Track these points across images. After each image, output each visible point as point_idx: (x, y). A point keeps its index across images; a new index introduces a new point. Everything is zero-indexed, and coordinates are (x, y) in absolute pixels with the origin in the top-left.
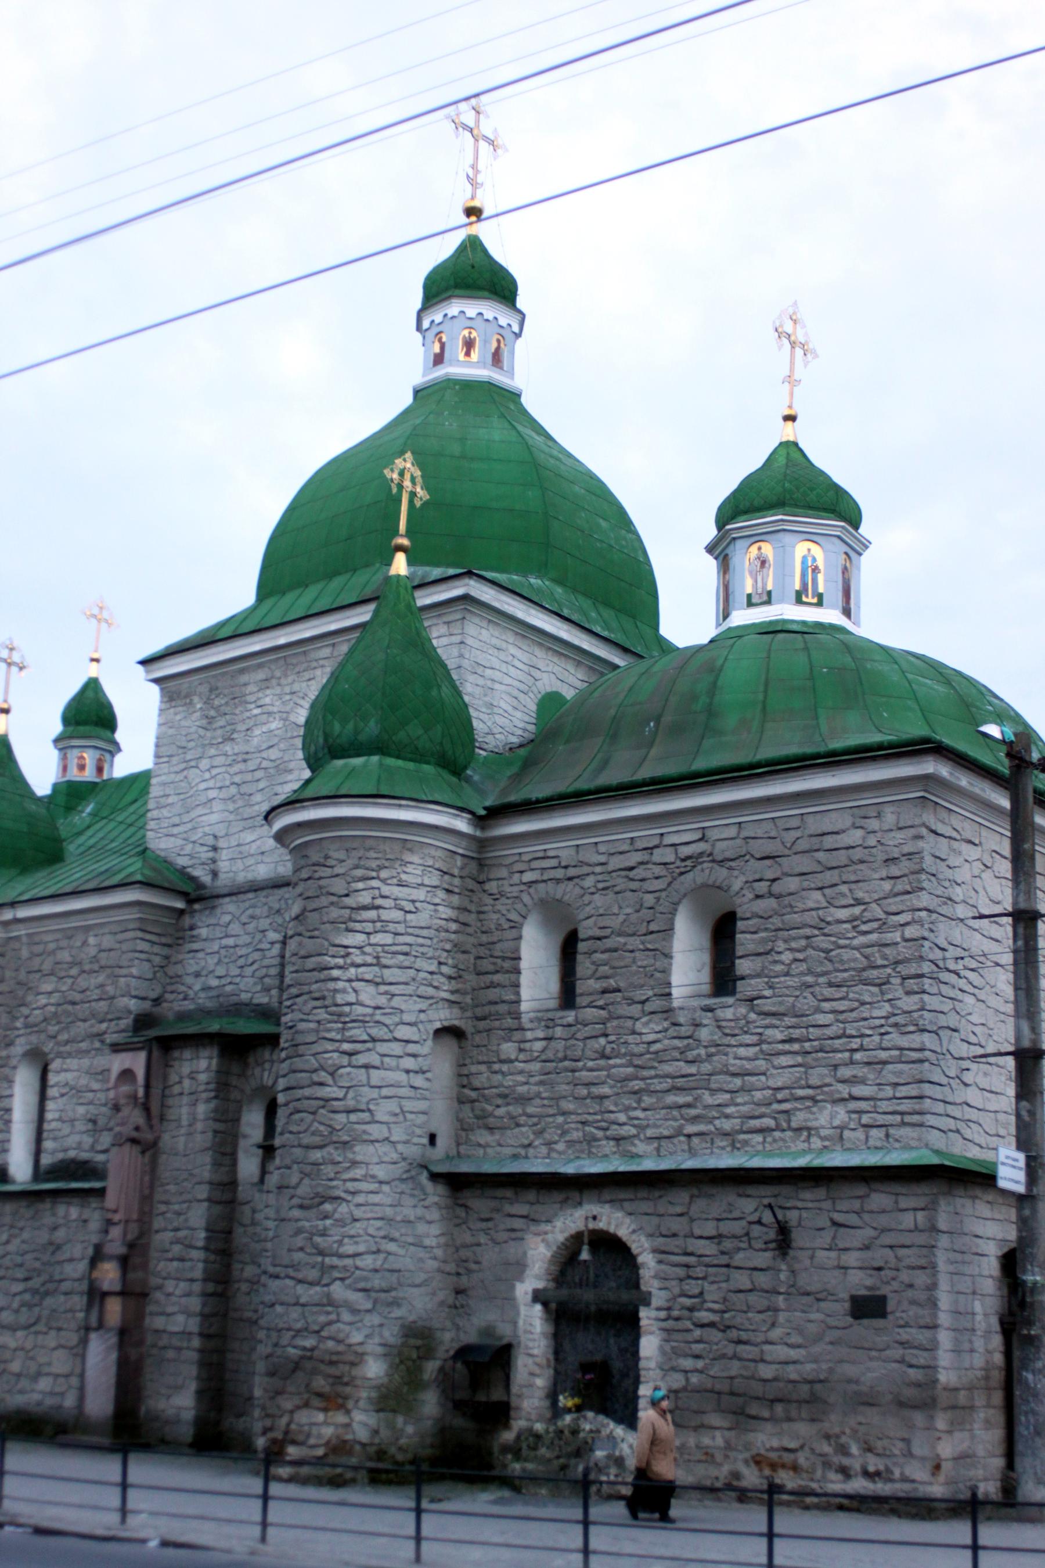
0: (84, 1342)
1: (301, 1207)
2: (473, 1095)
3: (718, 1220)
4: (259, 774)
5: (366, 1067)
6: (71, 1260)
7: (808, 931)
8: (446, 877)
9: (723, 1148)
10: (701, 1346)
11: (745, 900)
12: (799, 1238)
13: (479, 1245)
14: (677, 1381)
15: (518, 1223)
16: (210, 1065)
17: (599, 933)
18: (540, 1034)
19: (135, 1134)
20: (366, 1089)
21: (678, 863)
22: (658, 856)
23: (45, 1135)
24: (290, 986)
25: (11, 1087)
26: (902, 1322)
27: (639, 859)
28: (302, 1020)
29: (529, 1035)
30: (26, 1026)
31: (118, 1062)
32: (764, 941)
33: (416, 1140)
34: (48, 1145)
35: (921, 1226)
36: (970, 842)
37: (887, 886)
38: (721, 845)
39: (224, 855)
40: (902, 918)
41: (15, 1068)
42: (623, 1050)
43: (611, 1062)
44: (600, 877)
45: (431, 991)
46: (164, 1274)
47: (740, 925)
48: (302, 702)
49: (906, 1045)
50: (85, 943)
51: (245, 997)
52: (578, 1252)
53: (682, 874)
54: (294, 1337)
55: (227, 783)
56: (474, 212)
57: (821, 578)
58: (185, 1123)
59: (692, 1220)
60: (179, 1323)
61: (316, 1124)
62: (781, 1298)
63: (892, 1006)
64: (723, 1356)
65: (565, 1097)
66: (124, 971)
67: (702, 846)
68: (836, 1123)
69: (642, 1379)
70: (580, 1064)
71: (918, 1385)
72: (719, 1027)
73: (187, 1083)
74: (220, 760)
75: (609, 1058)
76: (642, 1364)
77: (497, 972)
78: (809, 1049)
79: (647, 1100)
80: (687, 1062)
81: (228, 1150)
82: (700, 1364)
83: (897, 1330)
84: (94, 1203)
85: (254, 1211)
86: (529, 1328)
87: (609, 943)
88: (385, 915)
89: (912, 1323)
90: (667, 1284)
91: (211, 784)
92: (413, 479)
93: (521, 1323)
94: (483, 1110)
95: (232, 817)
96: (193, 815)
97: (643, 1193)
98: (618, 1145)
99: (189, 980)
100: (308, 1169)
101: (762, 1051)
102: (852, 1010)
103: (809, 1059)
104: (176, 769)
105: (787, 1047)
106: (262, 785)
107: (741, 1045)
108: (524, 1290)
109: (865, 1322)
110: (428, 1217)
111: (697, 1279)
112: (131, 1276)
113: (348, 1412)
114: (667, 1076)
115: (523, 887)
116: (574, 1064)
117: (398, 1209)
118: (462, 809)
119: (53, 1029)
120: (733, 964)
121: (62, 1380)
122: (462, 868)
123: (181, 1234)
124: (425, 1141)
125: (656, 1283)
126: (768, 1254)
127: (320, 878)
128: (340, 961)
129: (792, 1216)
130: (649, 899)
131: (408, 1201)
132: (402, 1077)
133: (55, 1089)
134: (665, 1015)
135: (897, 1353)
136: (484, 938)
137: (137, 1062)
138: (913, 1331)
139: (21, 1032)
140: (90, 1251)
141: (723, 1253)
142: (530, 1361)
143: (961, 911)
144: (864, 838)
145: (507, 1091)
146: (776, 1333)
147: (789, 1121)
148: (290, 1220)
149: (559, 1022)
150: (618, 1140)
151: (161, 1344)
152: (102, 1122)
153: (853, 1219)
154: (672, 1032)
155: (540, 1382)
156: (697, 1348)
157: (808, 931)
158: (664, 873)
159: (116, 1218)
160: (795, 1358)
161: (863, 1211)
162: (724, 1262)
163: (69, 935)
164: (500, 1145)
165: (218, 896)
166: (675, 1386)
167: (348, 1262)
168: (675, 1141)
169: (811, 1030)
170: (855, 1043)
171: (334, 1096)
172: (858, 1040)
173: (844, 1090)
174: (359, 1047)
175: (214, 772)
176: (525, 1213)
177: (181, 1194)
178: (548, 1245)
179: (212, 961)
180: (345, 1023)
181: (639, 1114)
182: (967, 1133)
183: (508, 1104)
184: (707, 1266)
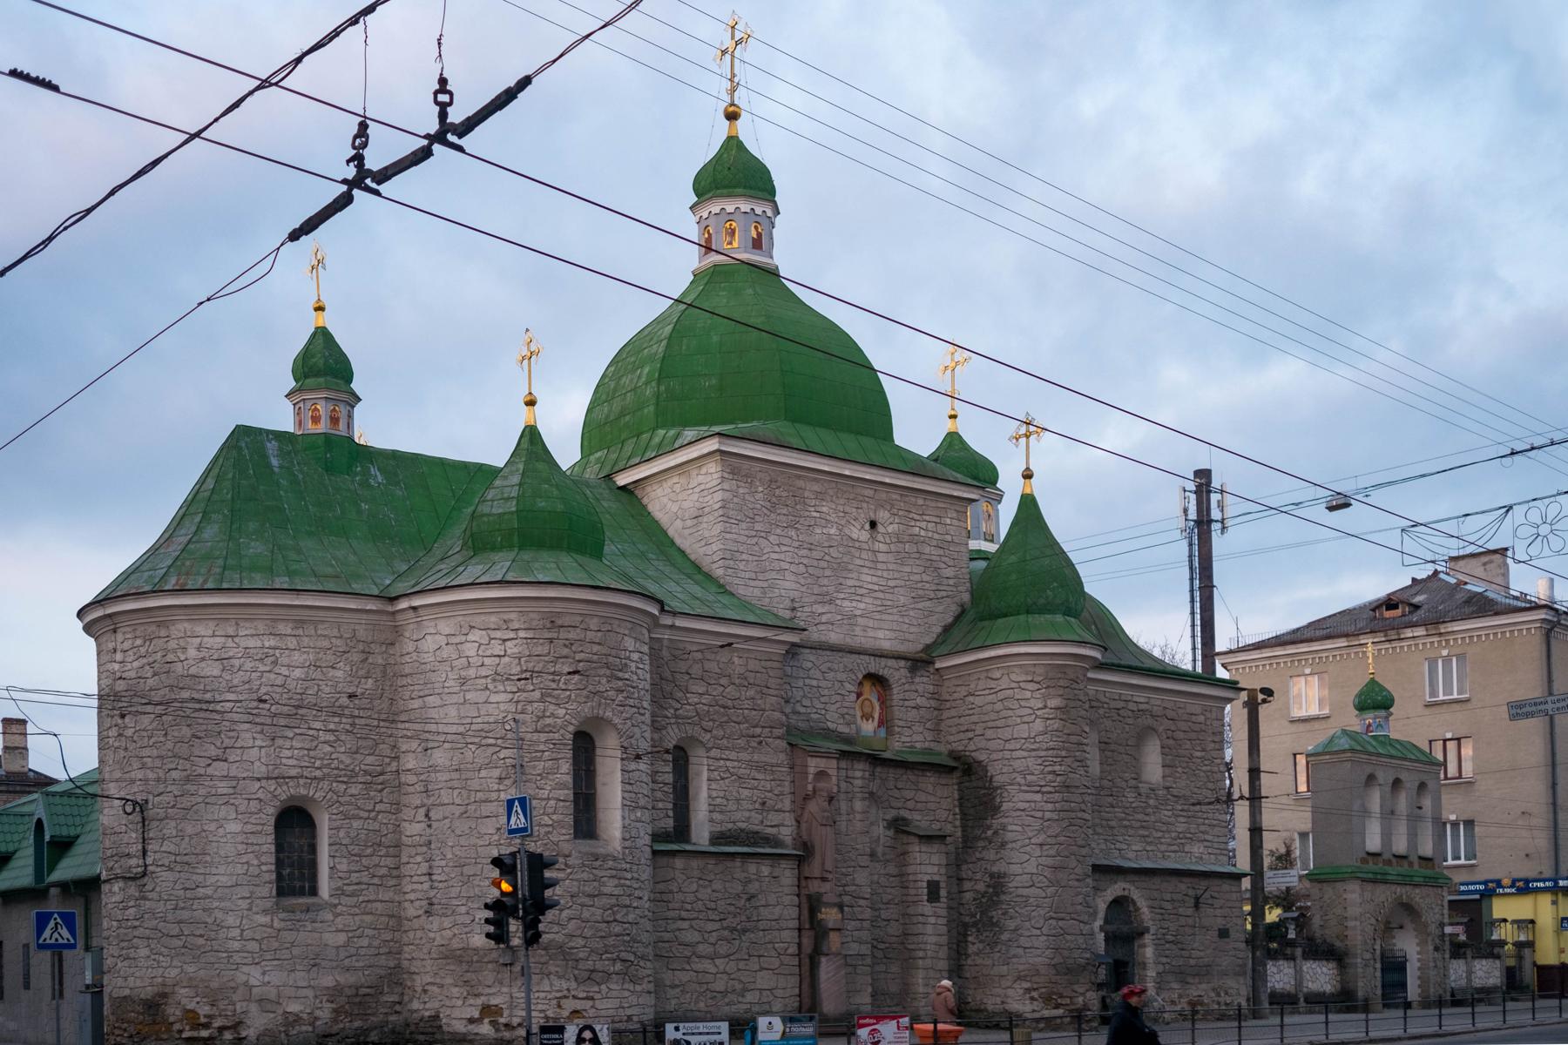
17: (1106, 740)
51: (829, 724)
70: (1102, 809)
79: (1131, 832)
84: (784, 864)
87: (1113, 747)
91: (782, 557)
95: (803, 589)
97: (1143, 878)
106: (828, 573)
114: (1139, 821)
123: (847, 888)
133: (716, 773)
152: (769, 803)
165: (799, 646)
175: (784, 548)
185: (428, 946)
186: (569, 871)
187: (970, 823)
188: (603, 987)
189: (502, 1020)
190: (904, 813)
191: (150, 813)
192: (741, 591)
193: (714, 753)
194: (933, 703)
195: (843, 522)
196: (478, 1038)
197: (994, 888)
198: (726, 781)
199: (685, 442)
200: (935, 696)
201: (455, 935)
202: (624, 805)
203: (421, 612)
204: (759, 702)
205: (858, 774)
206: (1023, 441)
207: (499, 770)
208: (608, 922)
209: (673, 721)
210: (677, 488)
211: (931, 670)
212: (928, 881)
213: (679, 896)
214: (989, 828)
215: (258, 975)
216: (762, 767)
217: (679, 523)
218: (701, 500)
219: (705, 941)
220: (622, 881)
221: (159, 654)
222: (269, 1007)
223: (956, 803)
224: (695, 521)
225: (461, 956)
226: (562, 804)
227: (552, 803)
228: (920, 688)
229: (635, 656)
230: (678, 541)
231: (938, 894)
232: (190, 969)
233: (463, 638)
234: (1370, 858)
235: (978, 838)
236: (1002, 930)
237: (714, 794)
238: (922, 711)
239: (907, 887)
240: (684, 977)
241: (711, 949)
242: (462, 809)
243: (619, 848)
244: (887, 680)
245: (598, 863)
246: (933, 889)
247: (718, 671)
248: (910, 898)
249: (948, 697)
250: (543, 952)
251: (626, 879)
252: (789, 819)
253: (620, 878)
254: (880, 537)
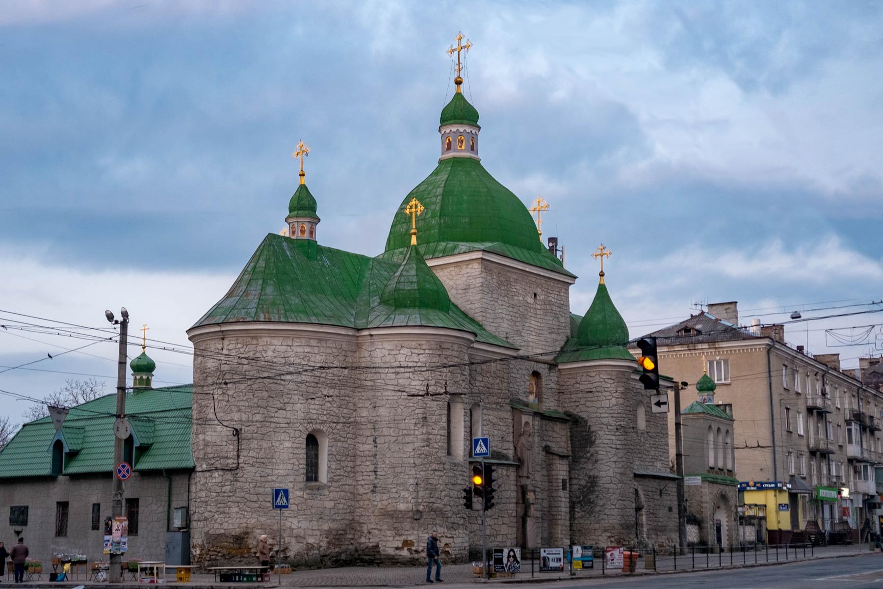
6: (505, 491)
106: (519, 320)
175: (504, 307)
185: (373, 509)
186: (445, 471)
187: (577, 450)
188: (457, 532)
189: (414, 548)
190: (549, 443)
191: (243, 435)
192: (488, 328)
193: (485, 411)
194: (557, 386)
195: (525, 294)
196: (401, 557)
197: (591, 483)
199: (462, 252)
200: (558, 383)
201: (389, 503)
202: (465, 439)
203: (374, 337)
204: (501, 386)
205: (536, 423)
206: (599, 257)
207: (415, 420)
208: (459, 498)
210: (453, 273)
211: (557, 370)
212: (562, 480)
214: (588, 452)
215: (296, 523)
216: (501, 419)
217: (454, 291)
218: (469, 281)
221: (252, 353)
222: (300, 540)
223: (568, 438)
224: (464, 291)
225: (393, 514)
226: (443, 437)
227: (439, 437)
228: (553, 378)
230: (453, 300)
231: (566, 486)
232: (262, 519)
233: (398, 352)
234: (711, 470)
235: (582, 457)
236: (596, 506)
237: (485, 432)
238: (553, 390)
239: (552, 482)
242: (395, 438)
243: (462, 460)
244: (540, 374)
245: (456, 468)
246: (564, 481)
248: (554, 488)
249: (564, 384)
250: (434, 513)
252: (512, 447)
254: (538, 302)
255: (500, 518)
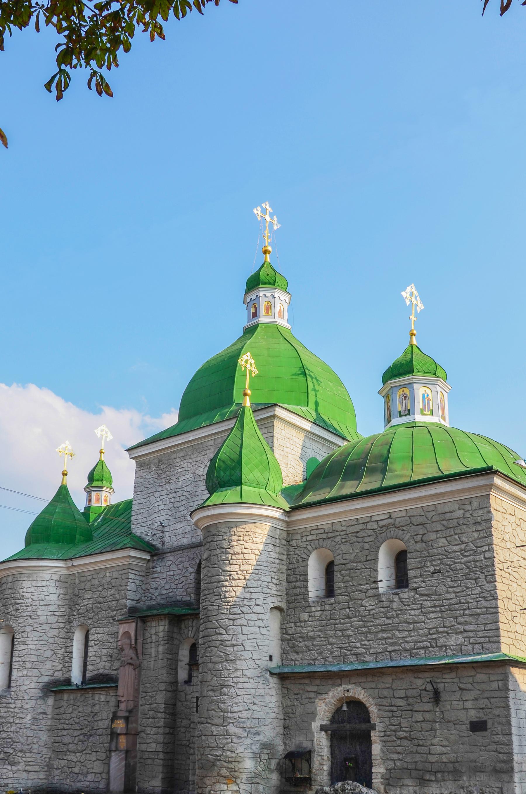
0: (109, 757)
1: (213, 690)
2: (289, 637)
3: (405, 689)
4: (182, 498)
5: (240, 625)
6: (102, 720)
7: (440, 557)
8: (273, 539)
9: (406, 657)
10: (401, 748)
11: (411, 544)
12: (444, 696)
13: (294, 705)
14: (390, 764)
15: (312, 695)
16: (164, 628)
17: (344, 562)
18: (319, 609)
19: (130, 661)
20: (241, 635)
21: (379, 529)
22: (369, 526)
23: (88, 663)
24: (204, 590)
25: (72, 642)
26: (495, 733)
27: (361, 528)
28: (211, 605)
29: (313, 609)
30: (78, 614)
31: (122, 629)
32: (420, 562)
33: (264, 658)
34: (89, 667)
35: (501, 688)
36: (511, 514)
37: (476, 535)
38: (398, 520)
39: (167, 534)
40: (484, 549)
41: (74, 633)
42: (357, 614)
43: (352, 620)
44: (343, 537)
45: (268, 591)
46: (145, 725)
47: (408, 555)
48: (201, 465)
49: (489, 606)
50: (105, 576)
51: (179, 598)
52: (342, 706)
53: (381, 533)
54: (211, 750)
55: (168, 502)
56: (266, 252)
57: (431, 402)
58: (153, 655)
59: (394, 690)
60: (153, 747)
61: (218, 652)
62: (437, 724)
63: (481, 588)
64: (412, 752)
65: (331, 637)
66: (123, 588)
67: (389, 521)
68: (458, 643)
69: (373, 764)
71: (503, 761)
72: (401, 602)
73: (154, 637)
74: (164, 492)
75: (351, 618)
76: (373, 758)
77: (297, 581)
78: (444, 610)
80: (387, 618)
81: (174, 667)
82: (401, 757)
83: (493, 736)
85: (186, 695)
86: (319, 743)
87: (348, 566)
88: (247, 556)
89: (500, 733)
90: (383, 720)
91: (160, 503)
92: (251, 364)
93: (315, 740)
94: (294, 644)
95: (170, 518)
96: (152, 517)
97: (370, 679)
98: (357, 657)
99: (152, 591)
100: (214, 673)
101: (421, 611)
102: (463, 591)
103: (444, 615)
104: (144, 497)
105: (434, 609)
106: (184, 502)
107: (412, 610)
108: (315, 725)
109: (477, 733)
110: (271, 694)
111: (397, 717)
112: (130, 726)
113: (238, 784)
115: (308, 543)
116: (334, 621)
117: (257, 690)
118: (279, 508)
119: (91, 615)
120: (406, 574)
121: (99, 775)
122: (280, 535)
123: (152, 706)
124: (268, 659)
125: (378, 720)
126: (430, 704)
127: (217, 541)
128: (228, 578)
129: (441, 686)
130: (366, 546)
131: (261, 686)
132: (258, 629)
134: (376, 597)
135: (493, 747)
136: (291, 566)
137: (131, 628)
138: (501, 736)
139: (76, 617)
140: (111, 715)
141: (409, 705)
142: (319, 758)
143: (509, 545)
144: (464, 514)
145: (304, 635)
146: (436, 741)
147: (436, 643)
148: (207, 697)
149: (327, 602)
150: (357, 655)
151: (144, 757)
153: (469, 686)
154: (379, 605)
155: (325, 768)
156: (399, 749)
157: (440, 557)
158: (373, 533)
159: (123, 699)
160: (445, 752)
161: (474, 682)
162: (409, 709)
163: (97, 572)
164: (302, 660)
165: (165, 553)
166: (389, 767)
167: (235, 715)
168: (384, 654)
169: (444, 601)
170: (465, 606)
171: (226, 639)
172: (467, 605)
173: (461, 628)
174: (237, 616)
176: (315, 690)
177: (152, 688)
178: (326, 704)
179: (163, 582)
180: (230, 606)
181: (367, 643)
182: (518, 645)
183: (305, 641)
184: (402, 711)
198: (97, 646)
204: (116, 596)
205: (161, 628)
209: (76, 617)
213: (64, 716)
219: (73, 743)
220: (8, 710)
229: (32, 590)
240: (63, 763)
241: (75, 747)
247: (98, 583)
251: (12, 708)
253: (8, 708)
255: (94, 754)
